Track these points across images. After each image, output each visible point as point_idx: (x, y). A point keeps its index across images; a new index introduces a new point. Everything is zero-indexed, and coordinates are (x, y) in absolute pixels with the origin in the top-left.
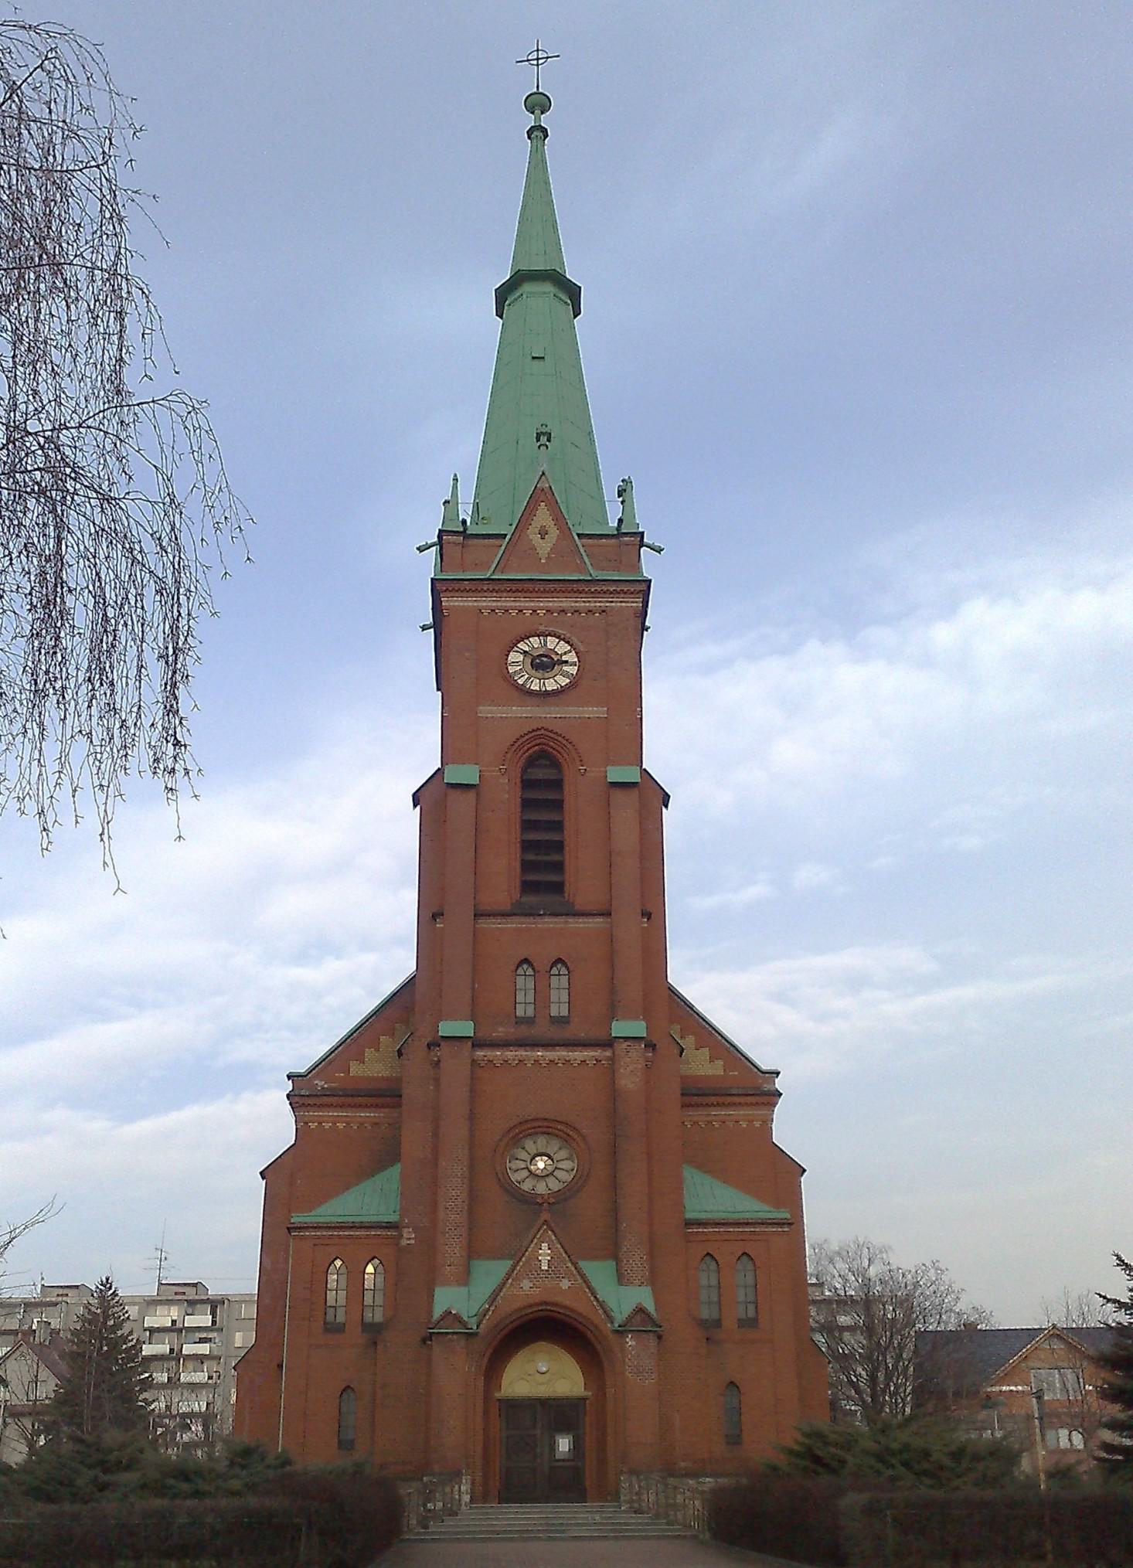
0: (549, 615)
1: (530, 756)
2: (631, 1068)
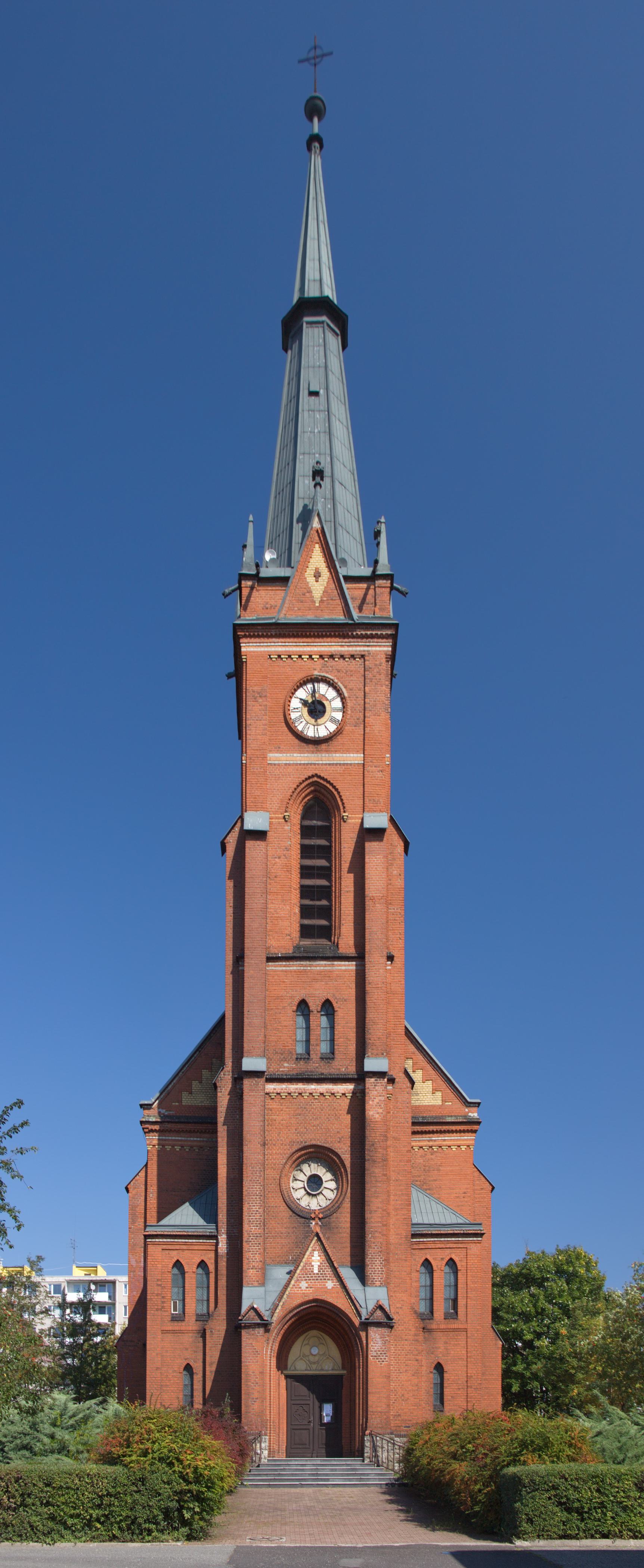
0: (321, 661)
2: (376, 1100)
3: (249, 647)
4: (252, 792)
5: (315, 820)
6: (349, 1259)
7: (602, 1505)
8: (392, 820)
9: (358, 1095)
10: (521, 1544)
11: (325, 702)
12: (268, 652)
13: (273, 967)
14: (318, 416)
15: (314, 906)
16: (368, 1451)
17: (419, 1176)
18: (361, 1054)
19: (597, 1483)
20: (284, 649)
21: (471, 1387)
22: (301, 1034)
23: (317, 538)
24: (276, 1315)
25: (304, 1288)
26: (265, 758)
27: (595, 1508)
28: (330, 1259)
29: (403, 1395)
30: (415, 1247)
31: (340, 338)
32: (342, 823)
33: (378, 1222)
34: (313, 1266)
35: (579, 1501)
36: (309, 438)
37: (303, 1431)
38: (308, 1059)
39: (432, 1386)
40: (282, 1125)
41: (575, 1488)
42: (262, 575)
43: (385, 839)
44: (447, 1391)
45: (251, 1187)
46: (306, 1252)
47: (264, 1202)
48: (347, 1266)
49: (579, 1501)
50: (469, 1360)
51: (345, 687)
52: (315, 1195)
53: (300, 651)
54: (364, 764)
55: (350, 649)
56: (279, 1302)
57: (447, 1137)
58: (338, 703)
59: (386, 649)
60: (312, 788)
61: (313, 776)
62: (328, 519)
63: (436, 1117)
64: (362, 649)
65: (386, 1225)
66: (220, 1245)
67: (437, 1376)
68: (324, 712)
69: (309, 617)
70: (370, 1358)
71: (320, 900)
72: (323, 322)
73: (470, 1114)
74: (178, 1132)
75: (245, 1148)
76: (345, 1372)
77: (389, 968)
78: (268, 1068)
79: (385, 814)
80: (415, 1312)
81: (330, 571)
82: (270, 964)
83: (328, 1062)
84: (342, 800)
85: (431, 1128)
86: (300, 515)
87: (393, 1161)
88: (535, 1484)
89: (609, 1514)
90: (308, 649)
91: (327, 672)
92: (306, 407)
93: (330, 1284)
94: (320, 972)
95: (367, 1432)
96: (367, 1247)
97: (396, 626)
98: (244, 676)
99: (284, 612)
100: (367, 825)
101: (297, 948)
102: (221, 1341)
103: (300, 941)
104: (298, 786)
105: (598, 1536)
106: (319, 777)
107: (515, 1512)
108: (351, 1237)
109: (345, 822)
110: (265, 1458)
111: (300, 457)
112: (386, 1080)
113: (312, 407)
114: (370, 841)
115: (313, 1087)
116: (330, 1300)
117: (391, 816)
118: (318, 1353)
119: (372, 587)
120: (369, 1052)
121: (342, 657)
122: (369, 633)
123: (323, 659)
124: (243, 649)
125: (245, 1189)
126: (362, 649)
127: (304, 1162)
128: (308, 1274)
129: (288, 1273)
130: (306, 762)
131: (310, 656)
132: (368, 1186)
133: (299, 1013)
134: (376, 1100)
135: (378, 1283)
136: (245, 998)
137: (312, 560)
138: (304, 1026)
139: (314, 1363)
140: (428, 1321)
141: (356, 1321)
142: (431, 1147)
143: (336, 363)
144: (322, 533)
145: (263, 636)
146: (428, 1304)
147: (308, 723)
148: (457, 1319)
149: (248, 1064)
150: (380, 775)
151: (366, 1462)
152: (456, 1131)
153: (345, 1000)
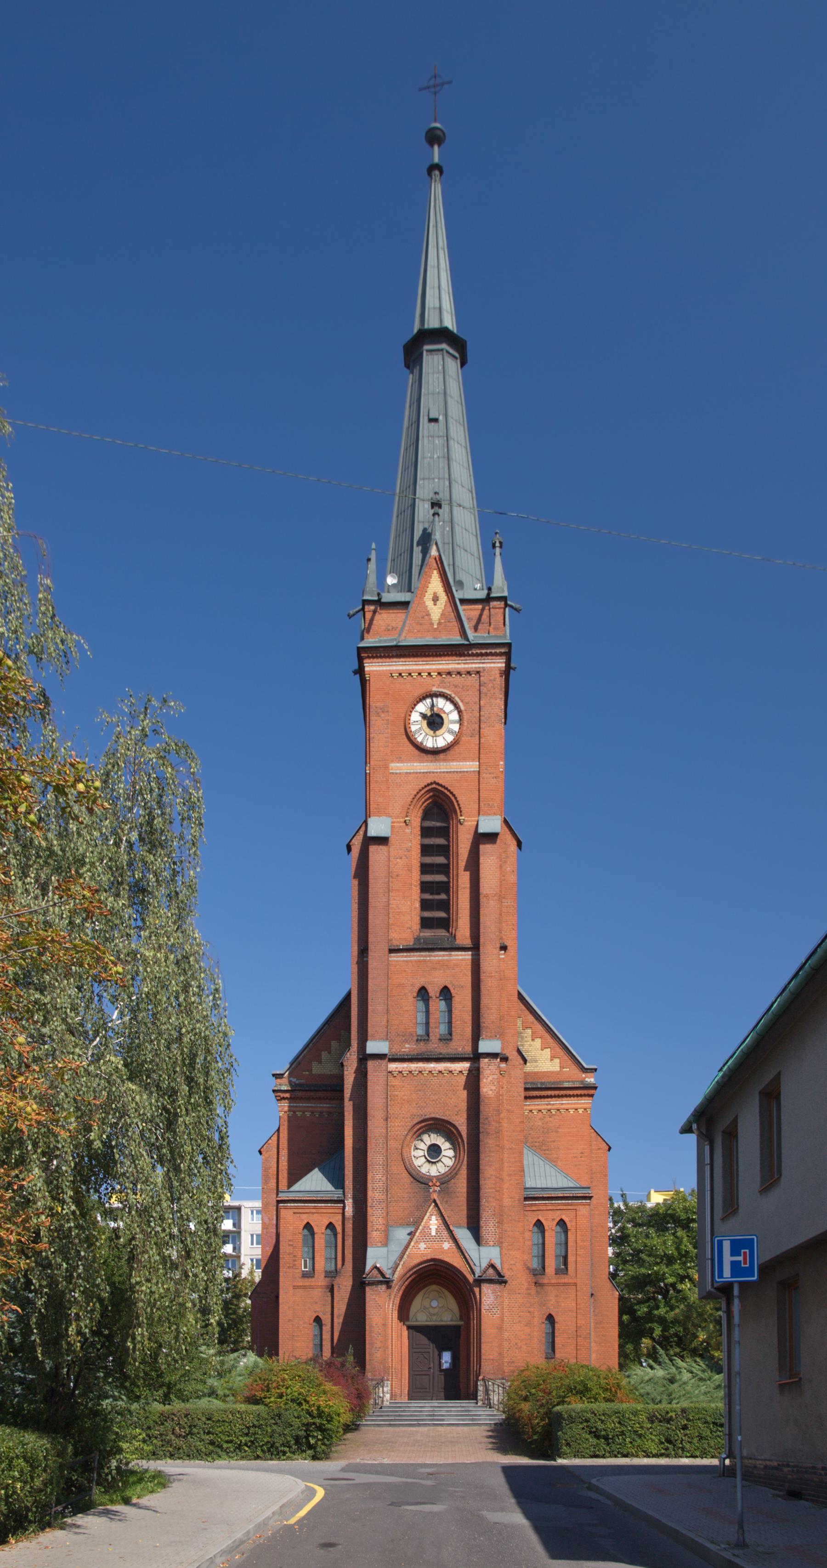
0: (439, 677)
1: (426, 807)
2: (490, 1079)
3: (372, 667)
4: (375, 799)
5: (434, 821)
6: (465, 1220)
7: (622, 1433)
8: (506, 822)
9: (474, 1072)
10: (560, 1461)
11: (443, 715)
12: (390, 670)
13: (395, 958)
14: (437, 442)
15: (433, 900)
16: (481, 1395)
17: (538, 1138)
18: (476, 1036)
19: (619, 1417)
20: (404, 668)
21: (580, 1336)
22: (421, 1018)
23: (435, 565)
24: (397, 1273)
25: (422, 1249)
26: (387, 768)
27: (617, 1435)
28: (446, 1223)
29: (516, 1344)
30: (528, 1208)
31: (459, 361)
32: (459, 825)
33: (491, 1188)
35: (605, 1430)
36: (429, 464)
37: (424, 1377)
38: (428, 1040)
39: (544, 1335)
40: (404, 1100)
41: (602, 1421)
42: (383, 600)
43: (498, 841)
44: (557, 1340)
45: (375, 1158)
46: (424, 1217)
47: (387, 1171)
48: (464, 1227)
49: (605, 1430)
50: (578, 1311)
51: (462, 701)
52: (435, 1163)
53: (419, 669)
54: (479, 772)
55: (466, 666)
56: (400, 1261)
57: (565, 1101)
58: (455, 716)
59: (500, 665)
60: (431, 794)
61: (432, 784)
62: (446, 541)
63: (554, 1083)
64: (477, 666)
65: (498, 1191)
66: (347, 1209)
67: (549, 1326)
68: (442, 724)
69: (427, 639)
70: (483, 1311)
71: (439, 894)
72: (442, 350)
73: (588, 1080)
75: (369, 1123)
76: (462, 1323)
77: (502, 956)
78: (390, 1049)
79: (499, 817)
80: (528, 1268)
81: (447, 595)
82: (392, 955)
84: (459, 805)
85: (549, 1093)
86: (420, 538)
87: (507, 1131)
88: (572, 1418)
89: (628, 1440)
90: (427, 667)
91: (445, 688)
92: (426, 434)
93: (447, 1245)
94: (439, 961)
95: (481, 1377)
96: (481, 1211)
97: (509, 645)
98: (368, 693)
99: (404, 634)
100: (481, 830)
101: (417, 939)
102: (348, 1295)
103: (420, 932)
104: (418, 793)
105: (619, 1456)
106: (438, 784)
107: (557, 1439)
108: (468, 1201)
109: (461, 824)
110: (387, 1401)
111: (420, 482)
112: (499, 1060)
113: (432, 433)
114: (484, 844)
115: (432, 1066)
116: (447, 1259)
117: (505, 818)
118: (438, 1306)
119: (487, 608)
120: (484, 1034)
121: (459, 673)
122: (483, 651)
123: (441, 675)
124: (367, 669)
125: (369, 1159)
126: (477, 666)
127: (424, 1133)
128: (426, 1234)
129: (409, 1234)
130: (426, 771)
131: (429, 674)
132: (482, 1156)
133: (419, 998)
134: (490, 1079)
135: (492, 1243)
136: (369, 988)
137: (430, 586)
138: (424, 1010)
139: (434, 1315)
140: (540, 1276)
141: (471, 1278)
142: (549, 1110)
143: (455, 388)
144: (440, 561)
145: (385, 657)
146: (540, 1261)
147: (427, 734)
148: (567, 1274)
149: (373, 1047)
150: (494, 781)
151: (479, 1404)
152: (574, 1096)
153: (462, 987)
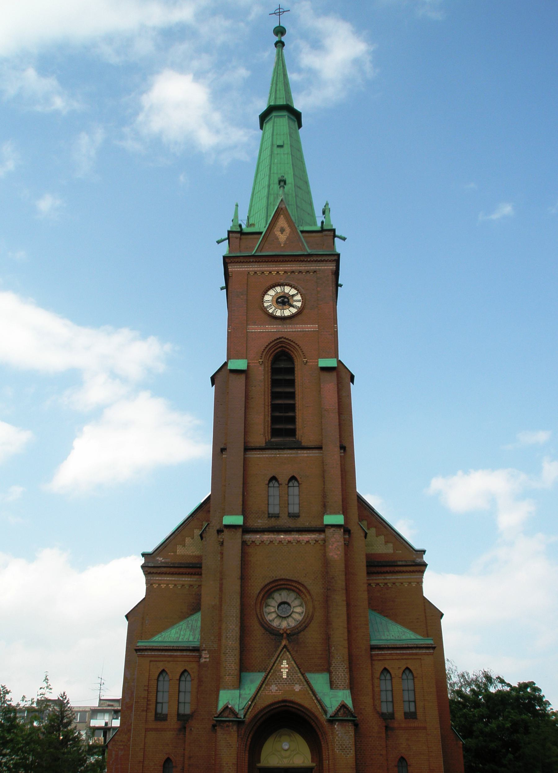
0: (286, 274)
1: (276, 354)
2: (334, 546)
25: (274, 691)
34: (282, 672)
74: (172, 574)
83: (295, 519)
103: (271, 438)
121: (300, 272)
134: (334, 546)
141: (323, 718)
